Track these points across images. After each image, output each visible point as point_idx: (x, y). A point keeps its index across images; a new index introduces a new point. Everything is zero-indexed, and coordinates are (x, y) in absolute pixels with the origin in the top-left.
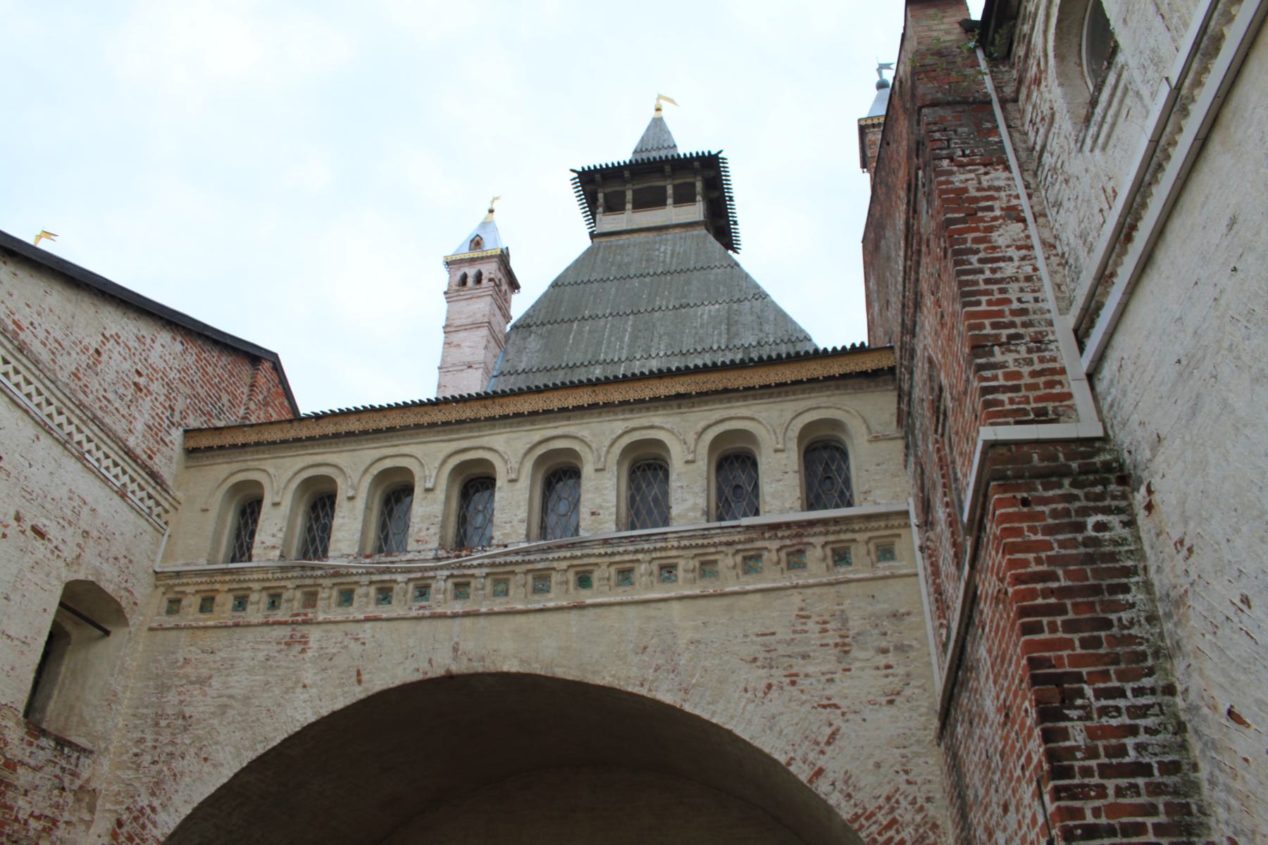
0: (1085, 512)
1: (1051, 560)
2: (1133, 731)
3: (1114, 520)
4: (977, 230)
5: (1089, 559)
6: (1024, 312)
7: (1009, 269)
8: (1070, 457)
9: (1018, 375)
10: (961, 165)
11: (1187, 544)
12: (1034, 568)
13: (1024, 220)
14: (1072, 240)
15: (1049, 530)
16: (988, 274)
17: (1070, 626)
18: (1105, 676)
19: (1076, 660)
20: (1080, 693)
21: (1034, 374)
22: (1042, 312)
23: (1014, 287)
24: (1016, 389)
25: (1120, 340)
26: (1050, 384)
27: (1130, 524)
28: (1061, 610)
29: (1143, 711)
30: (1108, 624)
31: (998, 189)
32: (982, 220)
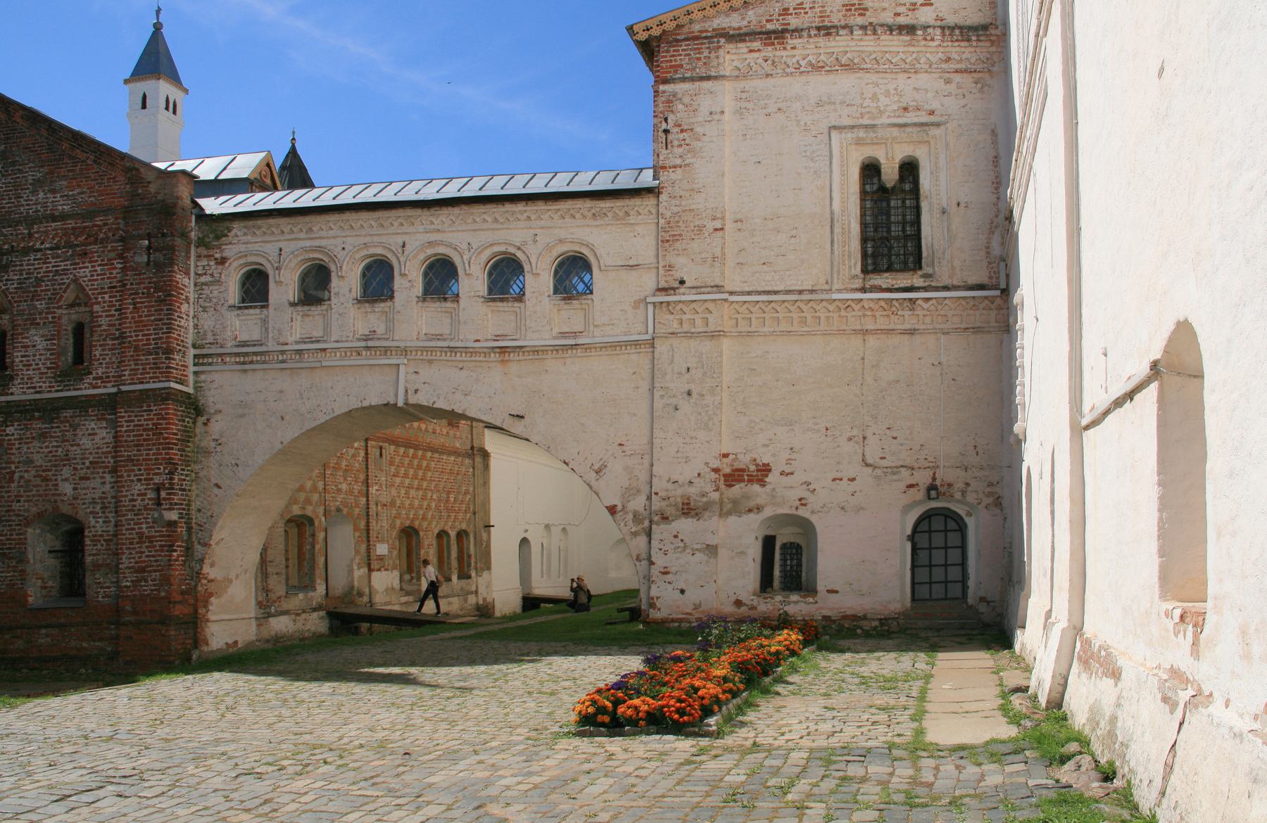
0: (186, 417)
1: (178, 430)
2: (184, 480)
3: (191, 421)
4: (178, 302)
5: (184, 431)
6: (182, 341)
7: (183, 323)
8: (182, 397)
9: (177, 364)
10: (180, 270)
11: (219, 442)
12: (175, 431)
13: (189, 303)
14: (206, 327)
15: (179, 420)
16: (178, 323)
17: (179, 450)
18: (182, 465)
19: (179, 460)
20: (177, 469)
21: (182, 366)
22: (186, 342)
23: (183, 330)
24: (177, 369)
25: (215, 376)
26: (184, 370)
27: (194, 423)
28: (176, 444)
29: (187, 475)
30: (184, 451)
31: (185, 286)
32: (180, 298)
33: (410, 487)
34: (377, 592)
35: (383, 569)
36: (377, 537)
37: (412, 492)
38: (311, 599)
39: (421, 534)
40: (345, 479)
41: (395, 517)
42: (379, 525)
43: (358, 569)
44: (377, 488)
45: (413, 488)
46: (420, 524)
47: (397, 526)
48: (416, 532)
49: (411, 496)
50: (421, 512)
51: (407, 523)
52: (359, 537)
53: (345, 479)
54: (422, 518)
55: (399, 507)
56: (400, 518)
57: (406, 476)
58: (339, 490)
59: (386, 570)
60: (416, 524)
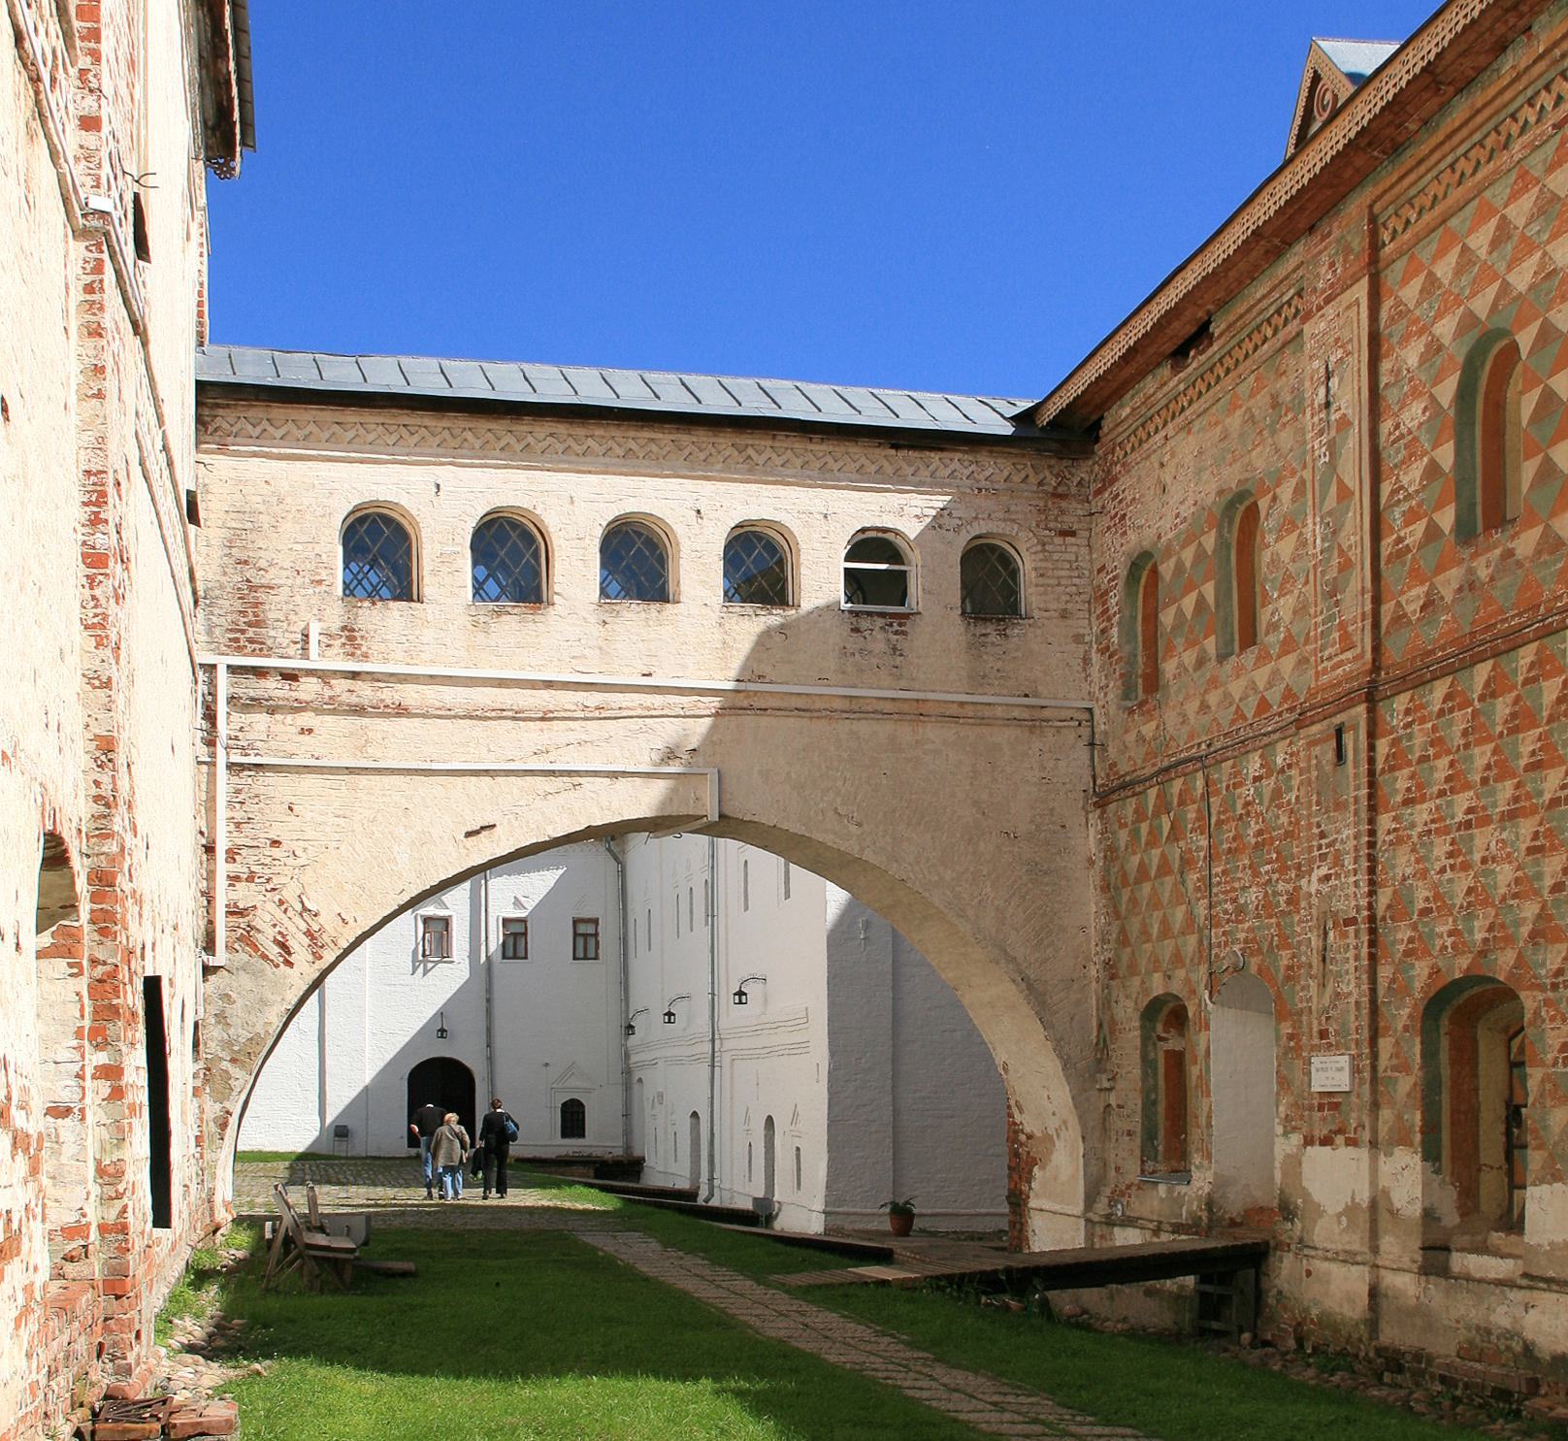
33: (1477, 818)
34: (1319, 1211)
35: (1340, 1139)
36: (1323, 1034)
37: (1484, 839)
38: (1178, 1201)
39: (1529, 1000)
40: (1256, 874)
41: (1408, 953)
42: (1329, 990)
43: (1285, 1134)
44: (1324, 871)
45: (1486, 821)
46: (1520, 956)
47: (1418, 985)
48: (1505, 994)
49: (1477, 857)
50: (1530, 910)
51: (1460, 967)
52: (1291, 1037)
53: (1256, 874)
54: (1534, 935)
55: (1425, 912)
56: (1427, 952)
57: (1456, 782)
58: (1241, 910)
59: (1352, 1142)
60: (1503, 963)
